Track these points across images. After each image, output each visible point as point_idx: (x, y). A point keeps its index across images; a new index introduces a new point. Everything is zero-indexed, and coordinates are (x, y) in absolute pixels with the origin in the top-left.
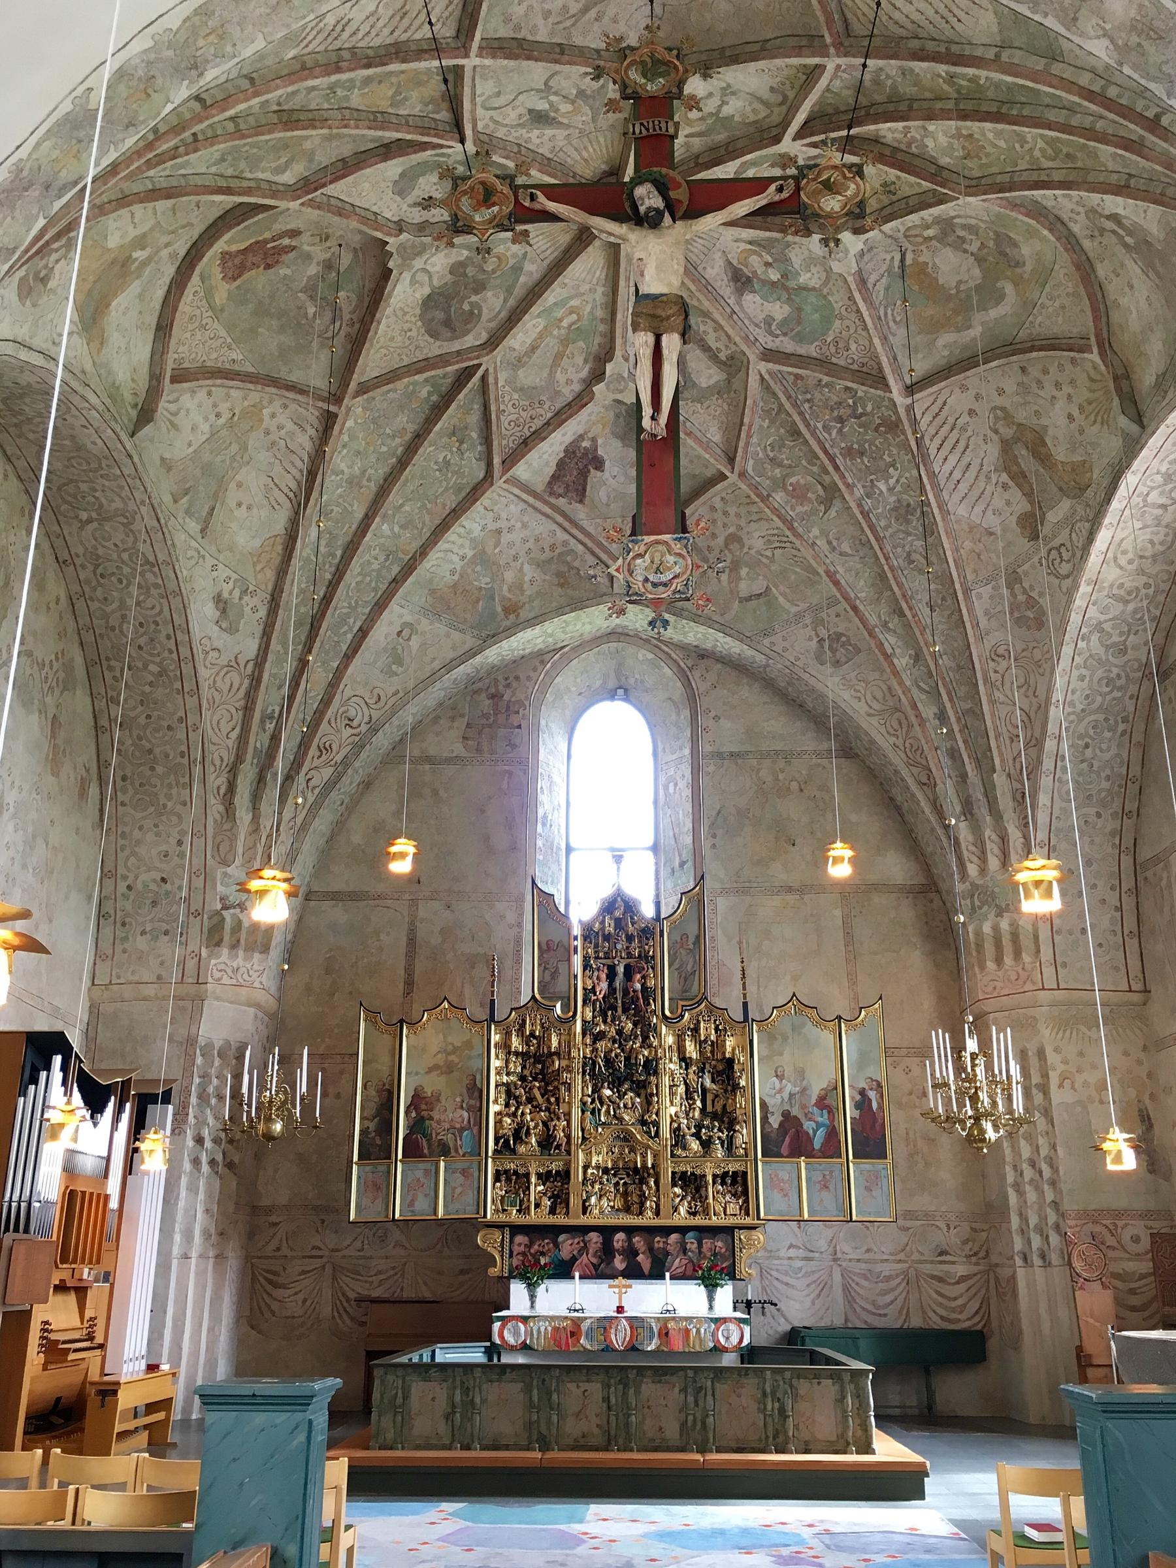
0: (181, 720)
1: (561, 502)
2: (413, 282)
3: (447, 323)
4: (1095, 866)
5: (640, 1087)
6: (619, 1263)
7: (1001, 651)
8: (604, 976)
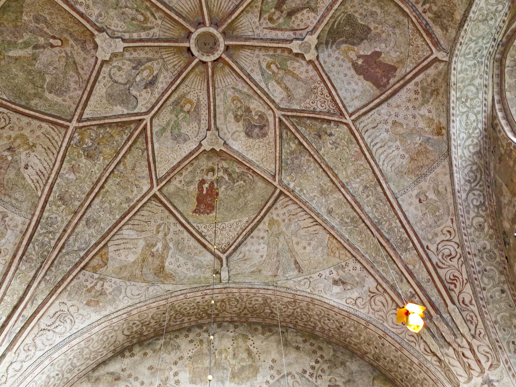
1: (392, 81)
2: (235, 140)
3: (261, 128)
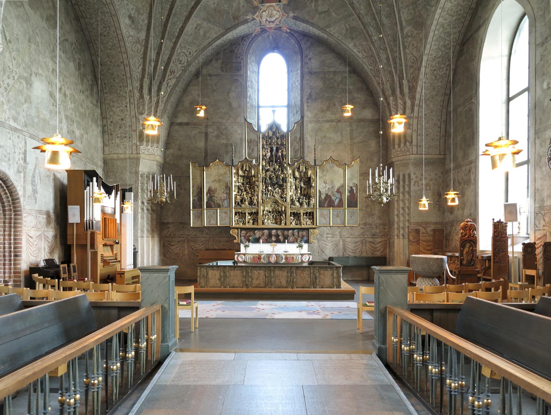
0: (121, 62)
4: (434, 113)
5: (282, 187)
6: (274, 239)
7: (409, 34)
8: (269, 151)
